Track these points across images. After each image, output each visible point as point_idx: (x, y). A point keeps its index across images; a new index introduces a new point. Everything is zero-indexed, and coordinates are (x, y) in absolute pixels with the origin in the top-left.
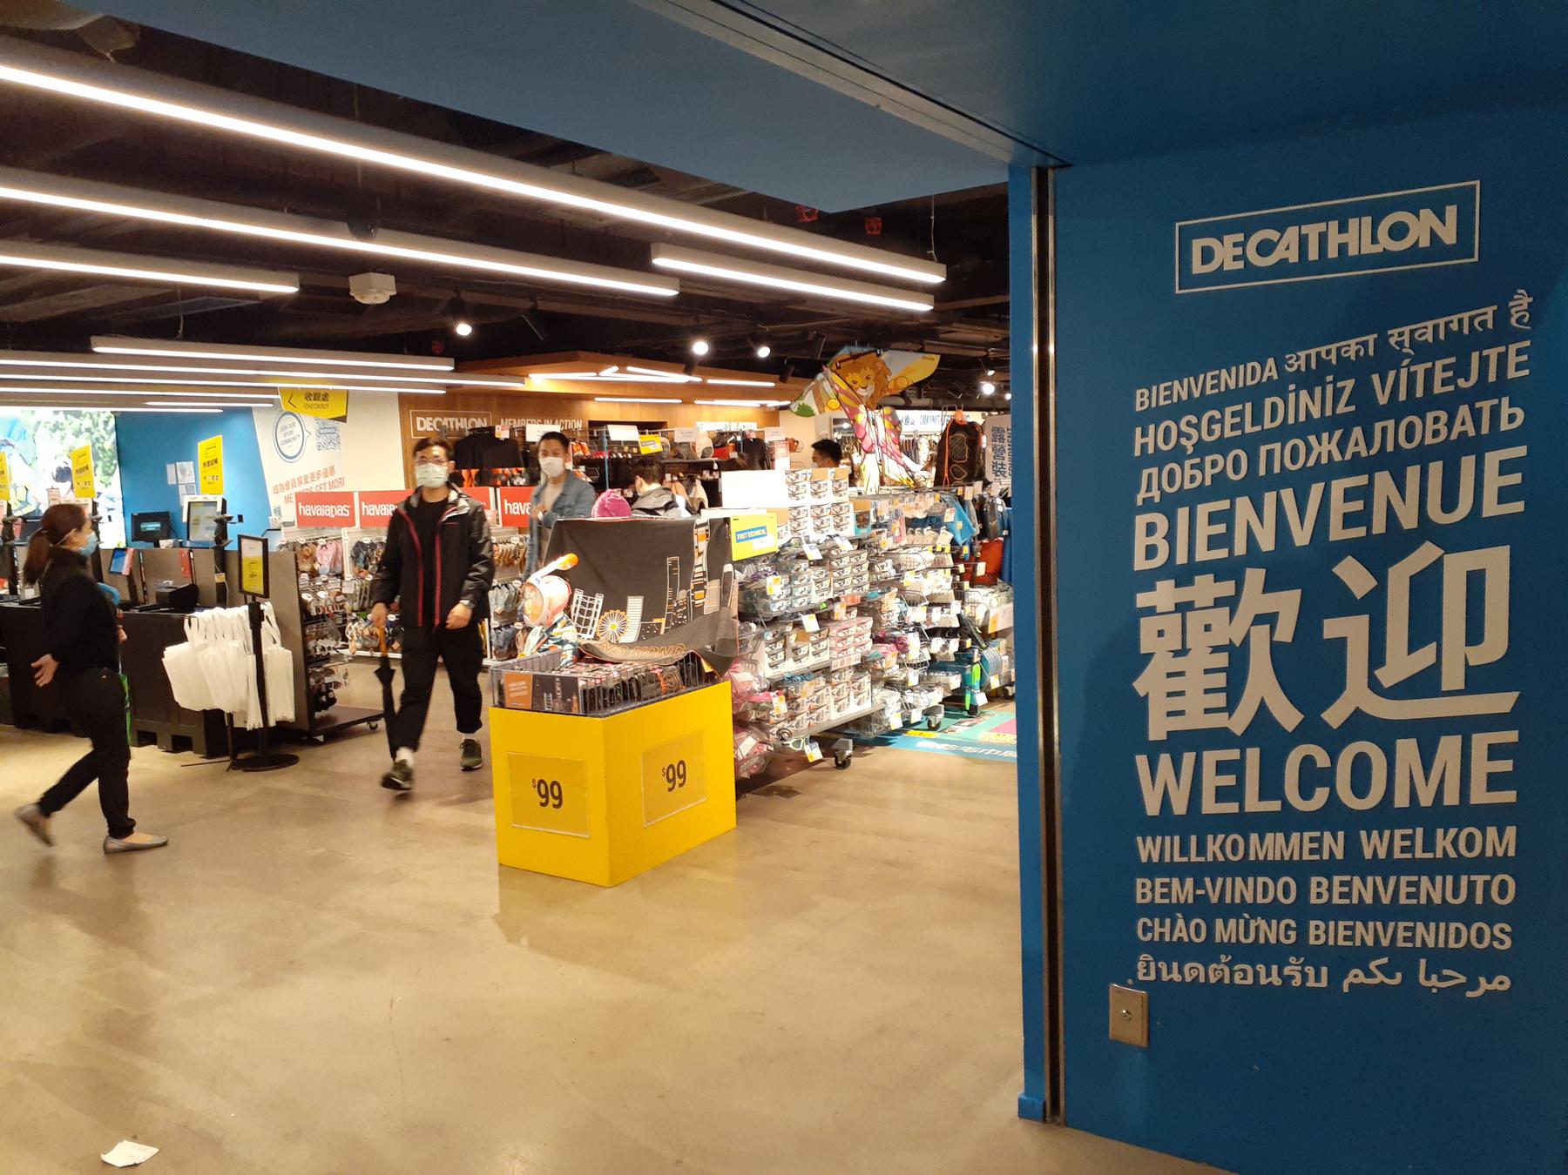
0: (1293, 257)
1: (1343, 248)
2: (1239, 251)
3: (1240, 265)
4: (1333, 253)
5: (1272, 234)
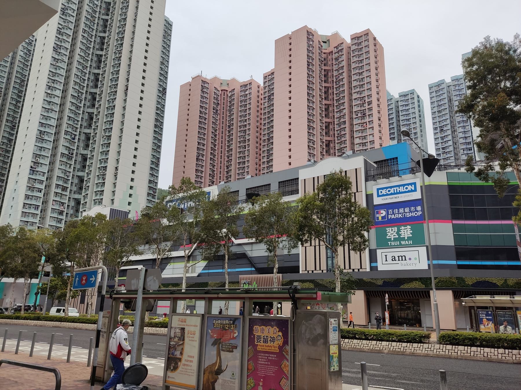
1: (399, 191)
4: (398, 191)
5: (390, 189)
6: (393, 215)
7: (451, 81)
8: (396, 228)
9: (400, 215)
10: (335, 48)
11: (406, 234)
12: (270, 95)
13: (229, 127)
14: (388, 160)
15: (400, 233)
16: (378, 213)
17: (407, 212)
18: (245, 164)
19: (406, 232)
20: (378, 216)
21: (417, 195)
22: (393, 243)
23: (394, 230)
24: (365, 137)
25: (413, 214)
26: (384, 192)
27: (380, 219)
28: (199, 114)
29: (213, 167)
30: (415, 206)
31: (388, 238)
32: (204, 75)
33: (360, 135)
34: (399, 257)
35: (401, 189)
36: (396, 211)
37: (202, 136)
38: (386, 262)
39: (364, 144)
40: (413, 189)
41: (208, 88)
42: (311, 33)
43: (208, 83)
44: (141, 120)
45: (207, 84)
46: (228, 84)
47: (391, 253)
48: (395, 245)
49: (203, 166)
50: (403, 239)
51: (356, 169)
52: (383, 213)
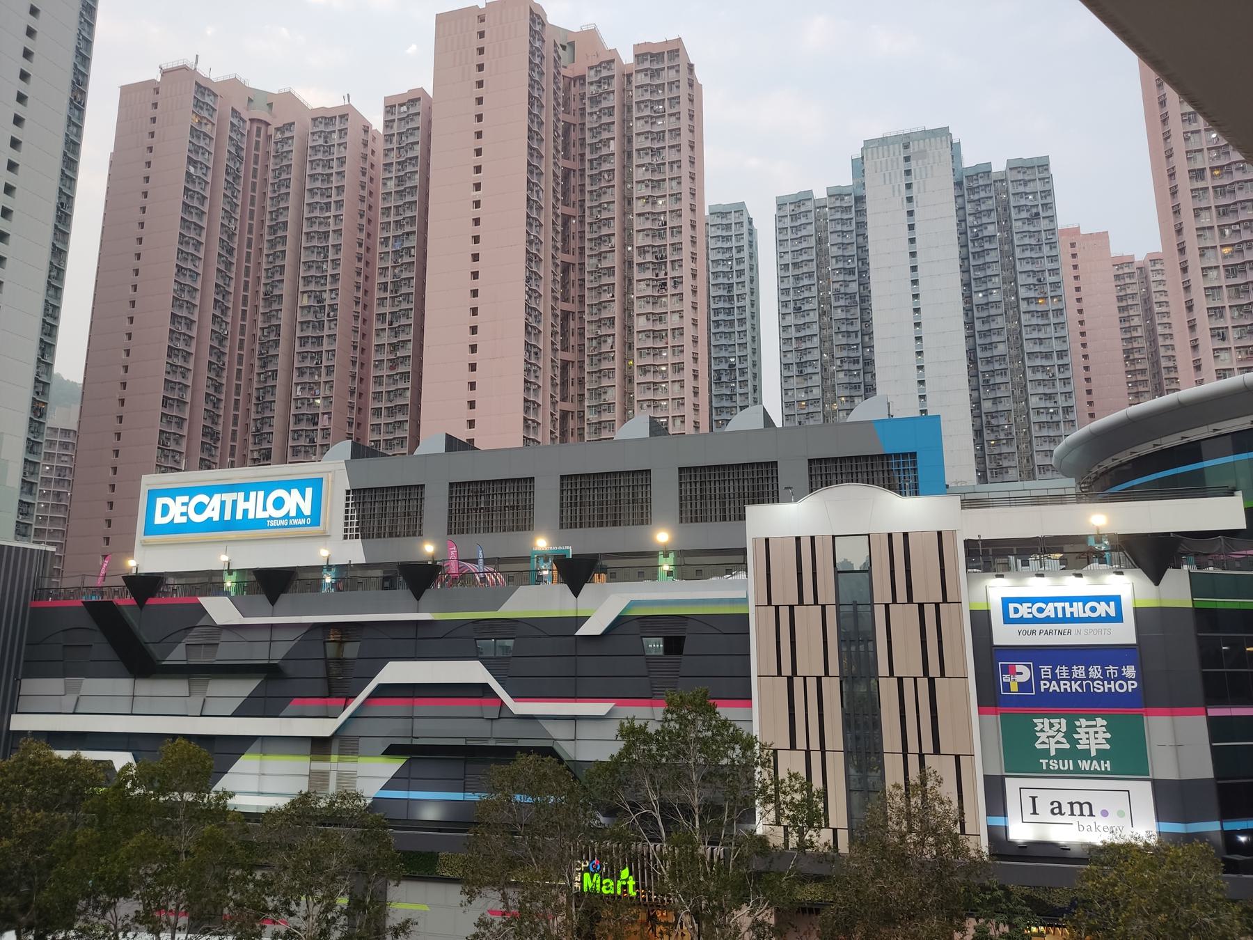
0: (1053, 616)
2: (1030, 610)
3: (1031, 616)
4: (1068, 615)
5: (1043, 605)
6: (1054, 683)
7: (826, 196)
8: (1063, 721)
9: (1075, 686)
10: (591, 68)
11: (1093, 741)
12: (404, 162)
13: (273, 229)
14: (888, 456)
15: (1076, 736)
16: (1006, 670)
17: (1097, 679)
18: (320, 344)
19: (1092, 734)
20: (1006, 678)
21: (1125, 634)
22: (1054, 765)
23: (1057, 727)
24: (660, 317)
25: (1112, 686)
26: (1024, 610)
27: (1014, 688)
28: (183, 184)
29: (220, 342)
30: (1120, 664)
31: (1038, 747)
32: (203, 70)
33: (649, 309)
34: (1071, 804)
35: (1077, 610)
36: (1063, 671)
37: (191, 250)
38: (1035, 819)
39: (657, 334)
40: (1113, 614)
41: (214, 110)
42: (539, 17)
43: (215, 95)
44: (17, 192)
45: (212, 97)
46: (270, 105)
47: (1049, 790)
48: (1059, 771)
49: (191, 338)
50: (1085, 754)
51: (939, 533)
52: (1024, 672)
